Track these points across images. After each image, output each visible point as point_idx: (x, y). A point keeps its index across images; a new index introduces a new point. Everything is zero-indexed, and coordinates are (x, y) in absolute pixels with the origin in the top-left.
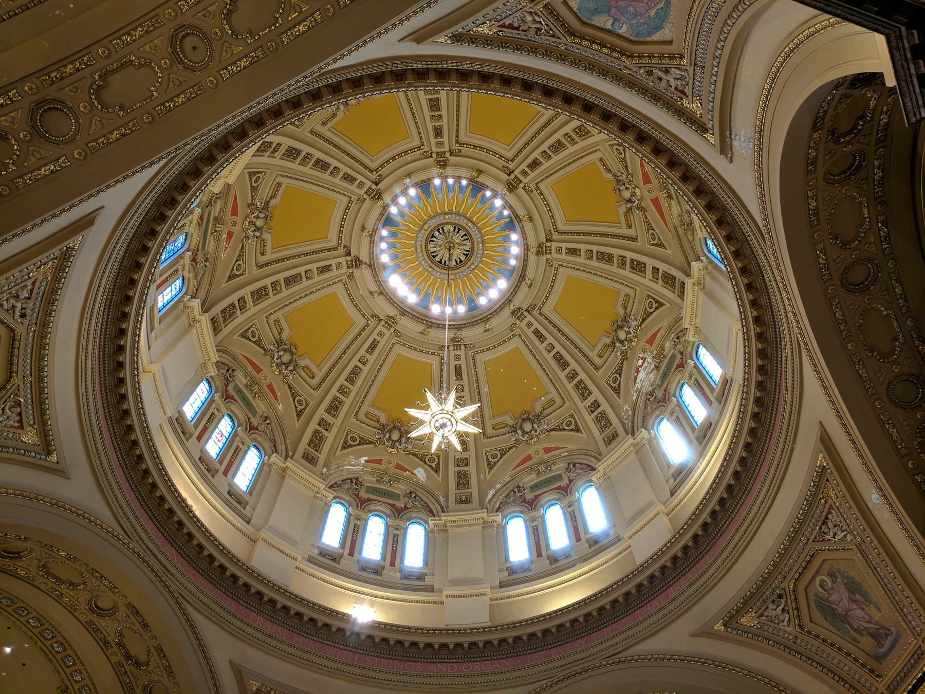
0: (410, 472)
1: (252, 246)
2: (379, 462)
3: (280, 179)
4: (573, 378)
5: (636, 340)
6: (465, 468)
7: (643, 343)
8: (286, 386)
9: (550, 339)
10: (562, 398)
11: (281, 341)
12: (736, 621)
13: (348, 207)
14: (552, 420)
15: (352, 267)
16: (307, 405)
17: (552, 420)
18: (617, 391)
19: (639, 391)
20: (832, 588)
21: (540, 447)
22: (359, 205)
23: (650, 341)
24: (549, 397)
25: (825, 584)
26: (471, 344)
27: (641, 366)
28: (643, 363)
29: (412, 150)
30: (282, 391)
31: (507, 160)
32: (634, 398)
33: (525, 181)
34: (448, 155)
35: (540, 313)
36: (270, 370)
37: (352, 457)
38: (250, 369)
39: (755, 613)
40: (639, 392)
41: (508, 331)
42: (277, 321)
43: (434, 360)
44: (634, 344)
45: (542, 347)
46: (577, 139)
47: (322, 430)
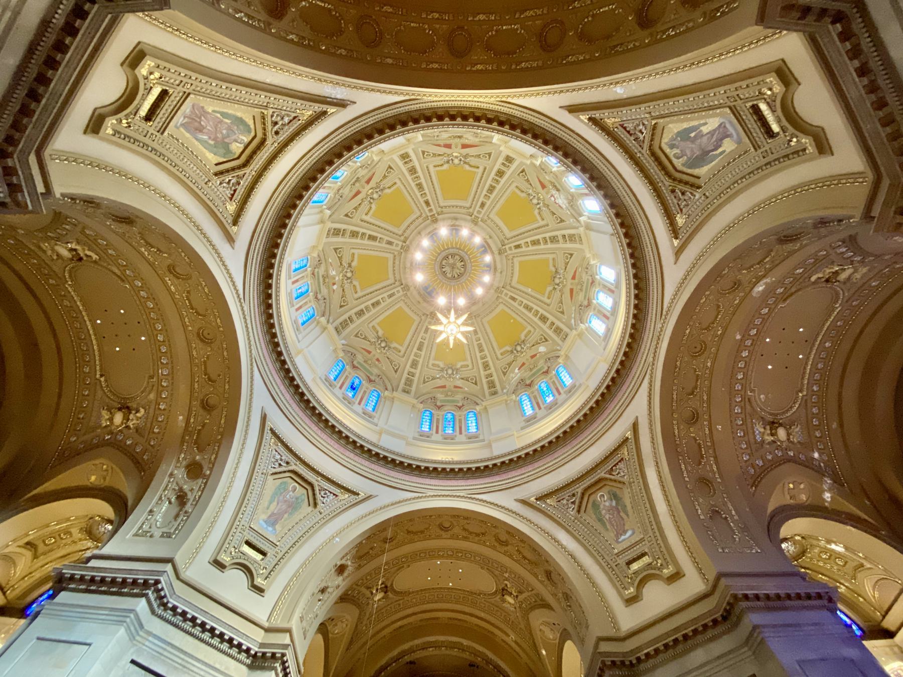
2: (523, 364)
3: (371, 325)
4: (546, 242)
7: (543, 192)
14: (561, 266)
17: (561, 266)
18: (562, 221)
19: (567, 208)
21: (570, 281)
23: (543, 187)
29: (394, 260)
31: (420, 216)
33: (435, 212)
34: (404, 244)
37: (511, 375)
42: (433, 365)
43: (501, 307)
46: (417, 175)
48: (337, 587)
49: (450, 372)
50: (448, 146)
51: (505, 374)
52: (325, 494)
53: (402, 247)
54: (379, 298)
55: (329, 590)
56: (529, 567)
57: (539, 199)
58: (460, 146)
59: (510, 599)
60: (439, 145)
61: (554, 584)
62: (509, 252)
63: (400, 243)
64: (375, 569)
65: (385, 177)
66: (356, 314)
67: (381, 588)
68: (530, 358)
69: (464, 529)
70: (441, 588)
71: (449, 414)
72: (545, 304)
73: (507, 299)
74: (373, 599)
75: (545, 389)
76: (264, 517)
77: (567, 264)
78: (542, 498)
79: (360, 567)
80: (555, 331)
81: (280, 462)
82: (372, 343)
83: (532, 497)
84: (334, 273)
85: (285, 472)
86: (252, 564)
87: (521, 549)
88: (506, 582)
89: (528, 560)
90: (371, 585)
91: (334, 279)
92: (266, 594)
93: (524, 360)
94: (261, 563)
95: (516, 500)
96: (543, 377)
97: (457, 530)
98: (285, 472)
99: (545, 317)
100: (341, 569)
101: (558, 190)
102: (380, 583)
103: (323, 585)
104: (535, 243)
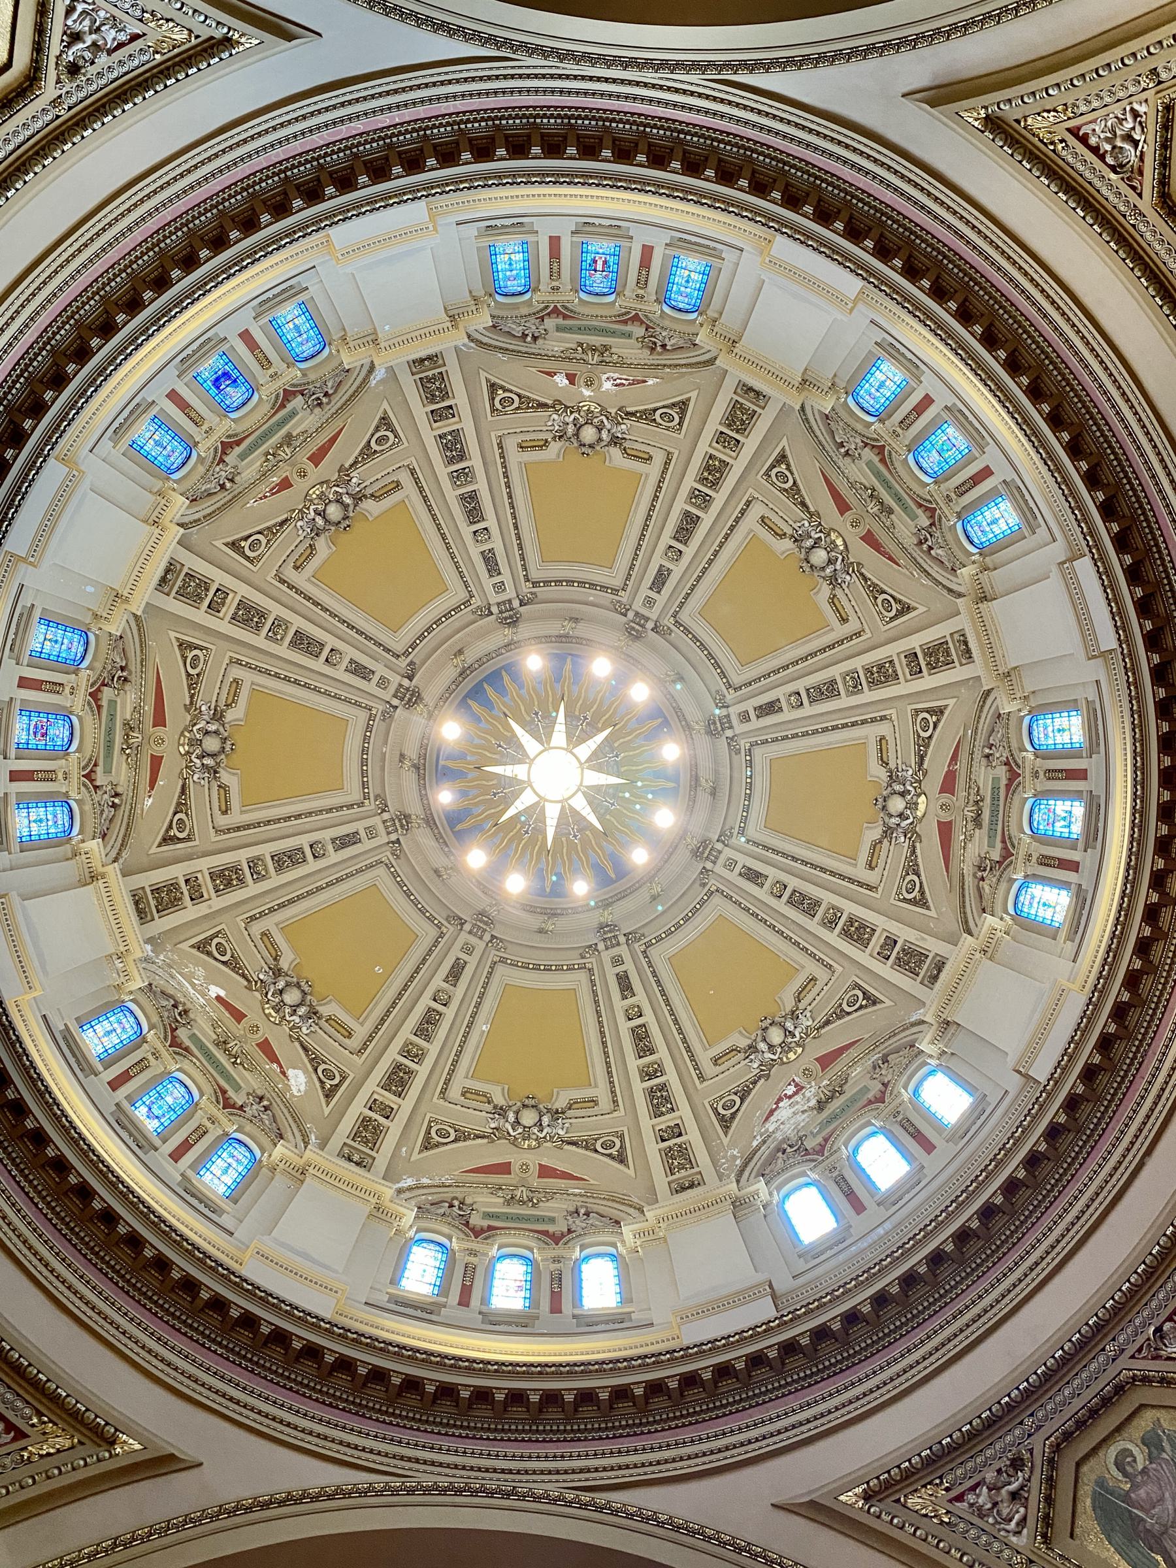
0: (281, 1067)
1: (295, 535)
2: (239, 1016)
4: (650, 1076)
5: (799, 1050)
6: (382, 1120)
8: (180, 783)
9: (640, 998)
10: (615, 1102)
11: (222, 716)
12: (896, 1497)
13: (457, 609)
15: (402, 699)
16: (188, 839)
18: (726, 1123)
20: (1145, 1471)
21: (534, 1160)
22: (473, 617)
23: (826, 1061)
24: (588, 1093)
25: (1129, 1459)
26: (501, 941)
27: (790, 1097)
28: (795, 1093)
29: (604, 588)
30: (168, 781)
32: (755, 1143)
35: (645, 952)
36: (177, 737)
38: (149, 708)
39: (947, 1489)
40: (769, 1136)
41: (576, 953)
44: (792, 1056)
45: (620, 1005)
47: (186, 893)
49: (212, 744)
50: (948, 785)
51: (202, 947)
53: (641, 618)
54: (491, 522)
57: (786, 1047)
58: (945, 817)
60: (954, 758)
62: (606, 956)
63: (653, 614)
65: (875, 591)
66: (455, 433)
68: (259, 1037)
72: (447, 1082)
73: (456, 953)
75: (169, 1100)
77: (589, 1145)
80: (365, 1122)
81: (89, 40)
82: (344, 473)
84: (607, 385)
85: (39, 47)
91: (589, 383)
93: (253, 1016)
96: (208, 1089)
98: (39, 47)
99: (403, 1083)
101: (821, 1106)
104: (642, 1040)
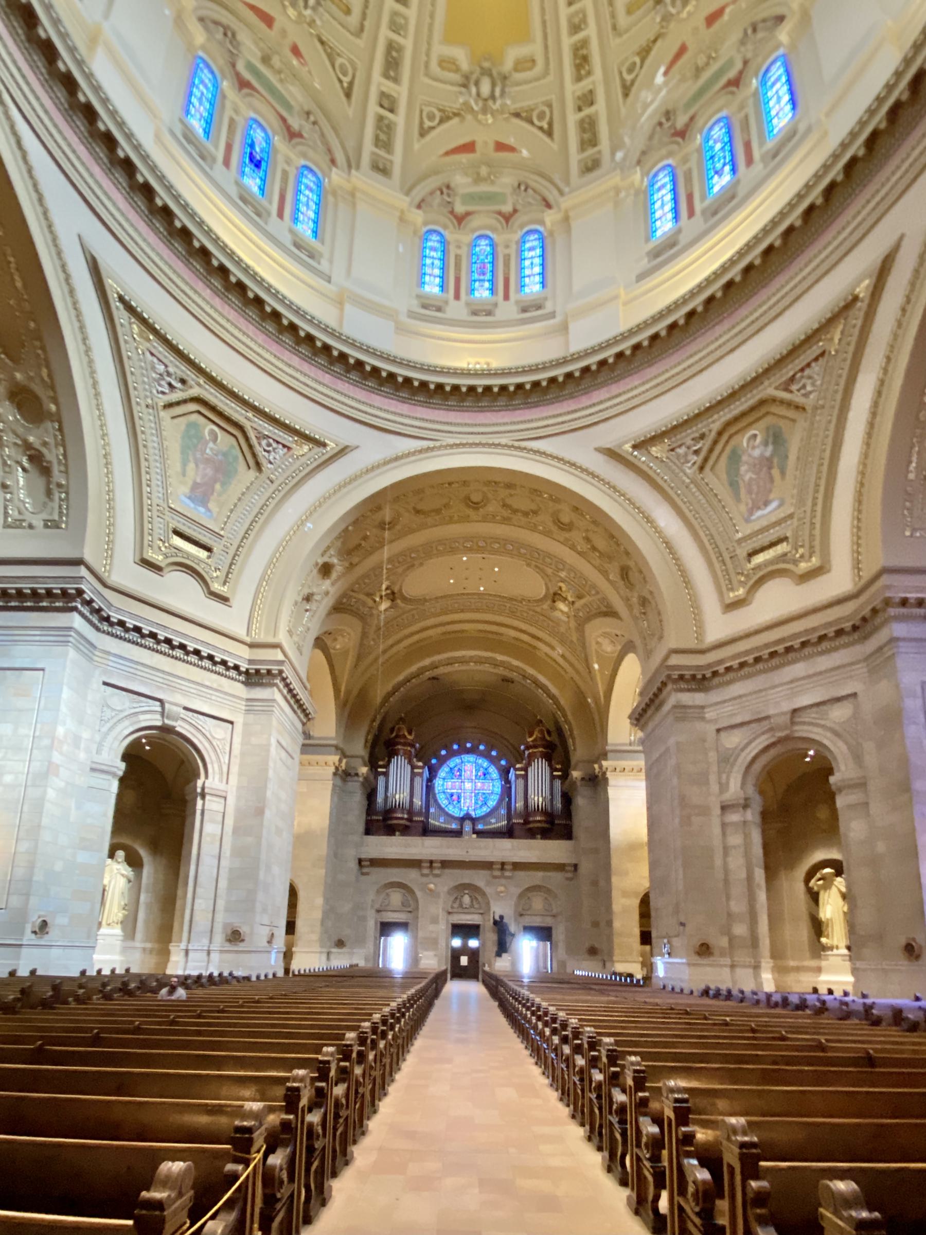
48: (327, 593)
52: (269, 445)
55: (317, 597)
56: (597, 562)
59: (562, 606)
61: (630, 585)
64: (374, 569)
67: (386, 595)
69: (505, 505)
70: (468, 594)
71: (483, 242)
74: (377, 609)
76: (185, 489)
78: (640, 445)
79: (352, 566)
83: (626, 442)
86: (198, 564)
87: (591, 535)
88: (562, 584)
89: (599, 552)
90: (371, 591)
92: (233, 602)
94: (209, 561)
95: (599, 450)
97: (491, 508)
100: (326, 570)
102: (384, 587)
103: (306, 591)
